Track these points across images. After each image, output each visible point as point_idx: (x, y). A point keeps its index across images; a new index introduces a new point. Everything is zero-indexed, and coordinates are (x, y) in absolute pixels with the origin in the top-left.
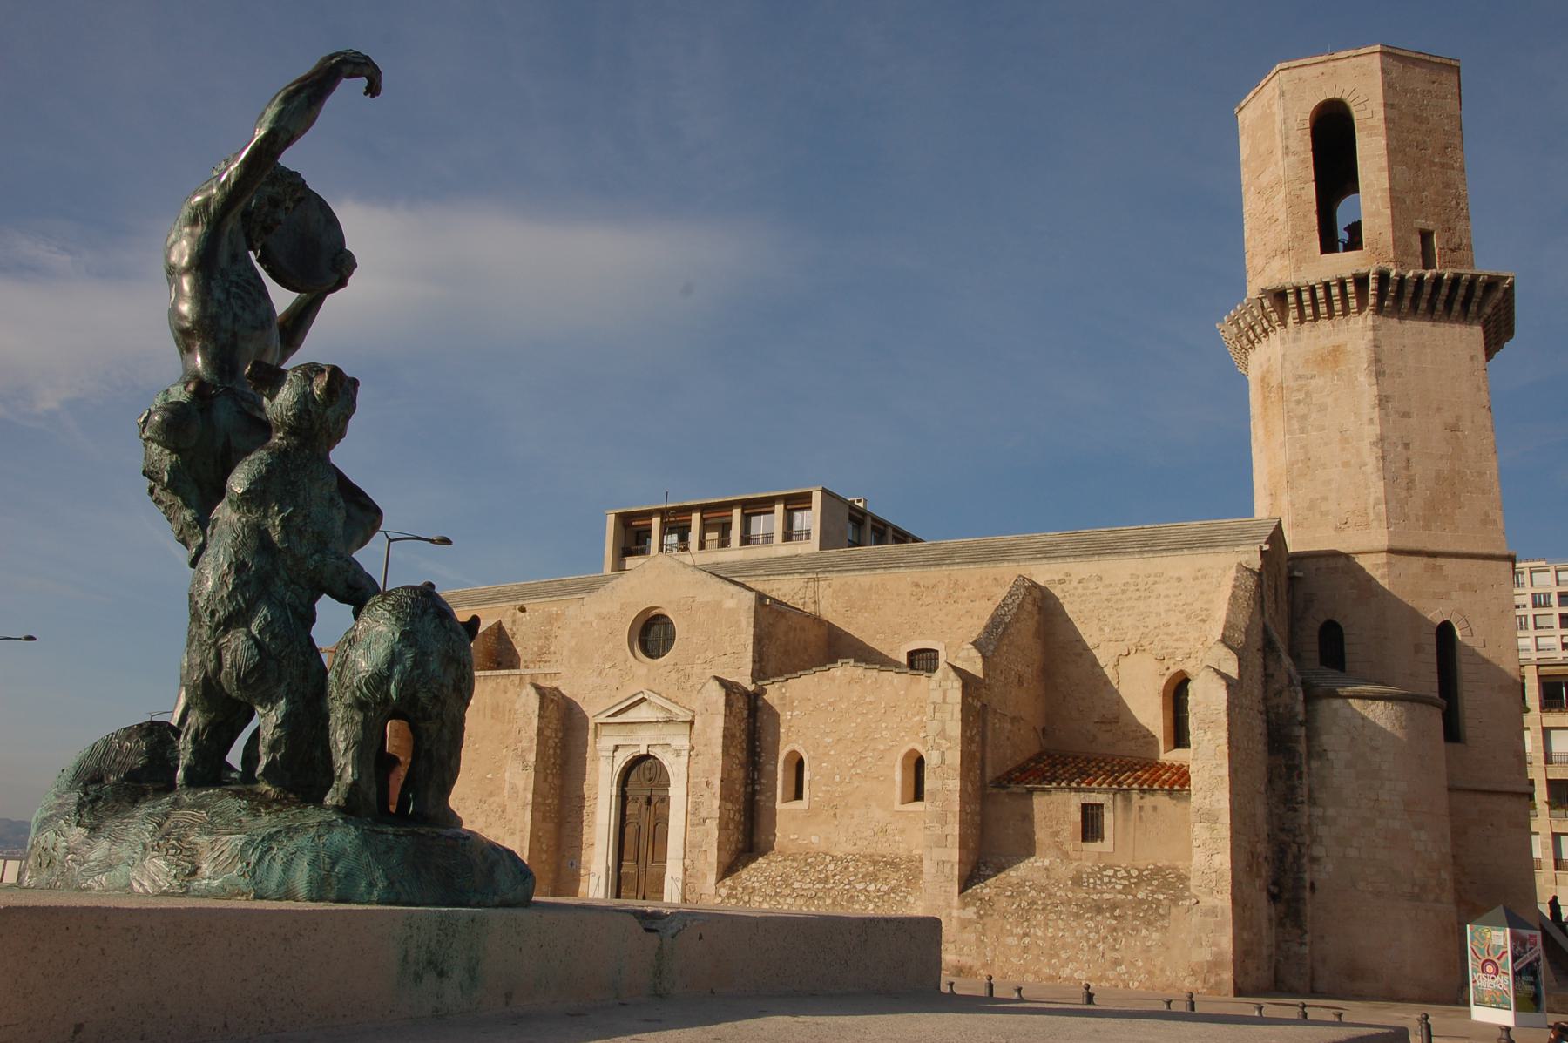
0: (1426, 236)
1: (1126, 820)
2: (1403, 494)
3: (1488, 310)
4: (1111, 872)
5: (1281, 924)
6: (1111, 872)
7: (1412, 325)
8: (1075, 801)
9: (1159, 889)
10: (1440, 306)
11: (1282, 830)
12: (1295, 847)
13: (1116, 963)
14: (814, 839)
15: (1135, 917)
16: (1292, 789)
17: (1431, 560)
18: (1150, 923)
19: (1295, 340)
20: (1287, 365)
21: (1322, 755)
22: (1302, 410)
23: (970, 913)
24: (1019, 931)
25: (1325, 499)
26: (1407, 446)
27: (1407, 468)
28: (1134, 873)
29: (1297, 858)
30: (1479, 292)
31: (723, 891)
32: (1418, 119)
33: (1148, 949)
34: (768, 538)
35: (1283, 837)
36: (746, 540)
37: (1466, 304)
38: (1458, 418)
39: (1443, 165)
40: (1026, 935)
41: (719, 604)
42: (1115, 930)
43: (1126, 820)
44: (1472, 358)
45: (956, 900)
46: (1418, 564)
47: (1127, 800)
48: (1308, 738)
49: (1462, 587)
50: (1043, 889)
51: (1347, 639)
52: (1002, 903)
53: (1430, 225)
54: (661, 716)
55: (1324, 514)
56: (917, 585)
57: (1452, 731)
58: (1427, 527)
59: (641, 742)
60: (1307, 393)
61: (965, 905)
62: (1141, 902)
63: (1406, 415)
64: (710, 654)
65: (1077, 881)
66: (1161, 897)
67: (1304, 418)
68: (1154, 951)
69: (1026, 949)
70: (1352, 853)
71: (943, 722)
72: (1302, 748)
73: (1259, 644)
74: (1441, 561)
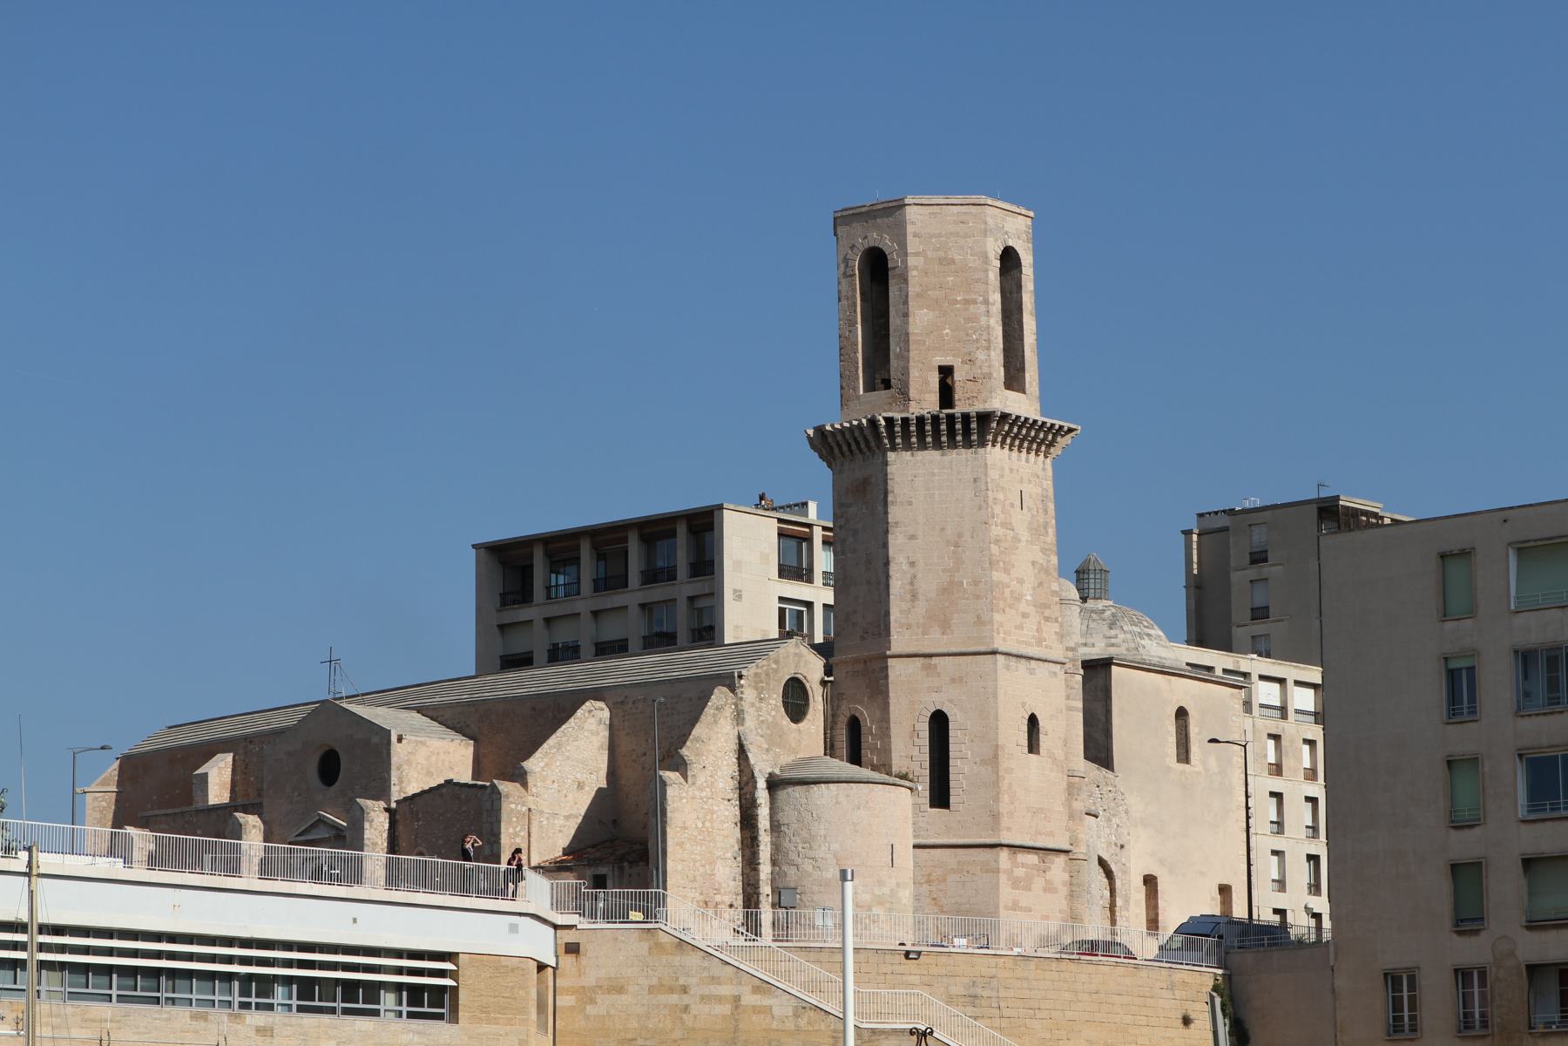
7: (921, 455)
17: (927, 660)
26: (912, 564)
27: (912, 584)
32: (946, 262)
34: (671, 575)
36: (652, 576)
38: (960, 536)
39: (967, 302)
46: (919, 662)
47: (621, 869)
49: (953, 681)
51: (864, 730)
57: (940, 796)
63: (912, 537)
73: (736, 747)
74: (935, 660)
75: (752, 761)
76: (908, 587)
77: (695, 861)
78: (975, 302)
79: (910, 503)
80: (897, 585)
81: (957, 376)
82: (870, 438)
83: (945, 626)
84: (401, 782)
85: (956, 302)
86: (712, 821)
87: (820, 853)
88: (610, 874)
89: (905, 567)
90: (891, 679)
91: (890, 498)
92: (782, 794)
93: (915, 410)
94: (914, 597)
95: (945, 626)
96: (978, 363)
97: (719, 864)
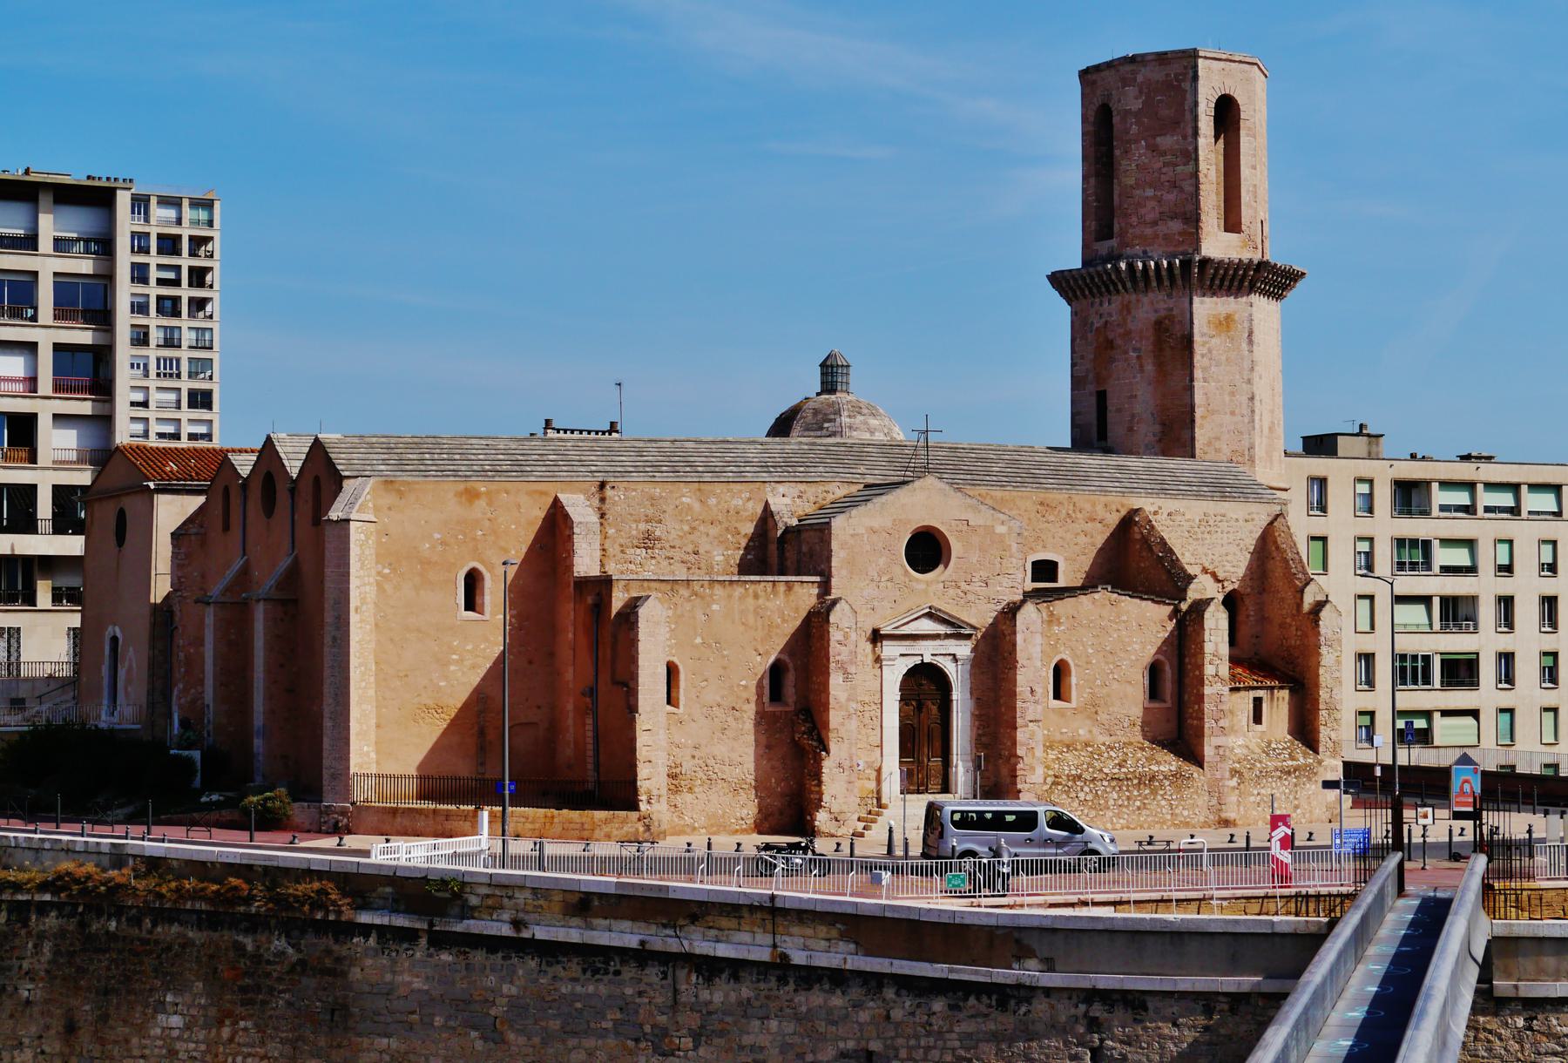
8: (1253, 694)
22: (1205, 361)
23: (1233, 783)
25: (1218, 439)
31: (1050, 780)
41: (989, 530)
45: (1227, 774)
54: (949, 631)
56: (1042, 504)
59: (927, 652)
60: (1210, 351)
64: (984, 574)
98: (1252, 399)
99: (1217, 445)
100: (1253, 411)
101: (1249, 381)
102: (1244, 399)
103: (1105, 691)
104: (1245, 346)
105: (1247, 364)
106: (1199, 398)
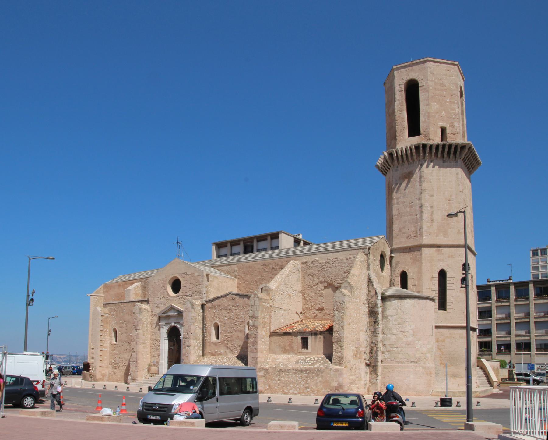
0: (443, 130)
1: (315, 342)
2: (429, 225)
3: (463, 156)
4: (309, 359)
5: (371, 374)
6: (309, 359)
9: (322, 364)
10: (445, 156)
11: (372, 343)
12: (375, 348)
13: (306, 388)
14: (222, 351)
15: (313, 373)
16: (375, 329)
18: (318, 375)
19: (396, 170)
20: (394, 180)
21: (384, 317)
24: (277, 379)
25: (404, 228)
26: (432, 207)
27: (431, 215)
28: (316, 359)
29: (376, 352)
30: (459, 150)
33: (317, 383)
35: (372, 345)
37: (455, 153)
38: (451, 196)
40: (279, 380)
42: (307, 377)
43: (315, 342)
44: (457, 174)
48: (382, 312)
50: (286, 365)
52: (270, 370)
53: (444, 125)
55: (404, 233)
58: (437, 236)
61: (260, 371)
62: (316, 368)
63: (432, 196)
65: (297, 362)
66: (322, 366)
67: (398, 199)
68: (319, 384)
69: (279, 385)
70: (395, 349)
71: (254, 312)
72: (380, 316)
75: (375, 287)
76: (430, 217)
77: (354, 332)
78: (454, 103)
79: (431, 182)
80: (425, 216)
81: (448, 131)
82: (414, 154)
83: (446, 234)
84: (207, 293)
85: (447, 102)
86: (359, 313)
87: (406, 329)
88: (310, 337)
89: (429, 208)
90: (423, 255)
91: (422, 179)
92: (388, 303)
93: (431, 142)
94: (432, 220)
95: (446, 234)
96: (455, 127)
97: (361, 333)
98: (421, 206)
99: (404, 231)
100: (422, 212)
101: (420, 199)
102: (417, 208)
103: (230, 334)
104: (417, 184)
105: (418, 192)
106: (395, 212)
